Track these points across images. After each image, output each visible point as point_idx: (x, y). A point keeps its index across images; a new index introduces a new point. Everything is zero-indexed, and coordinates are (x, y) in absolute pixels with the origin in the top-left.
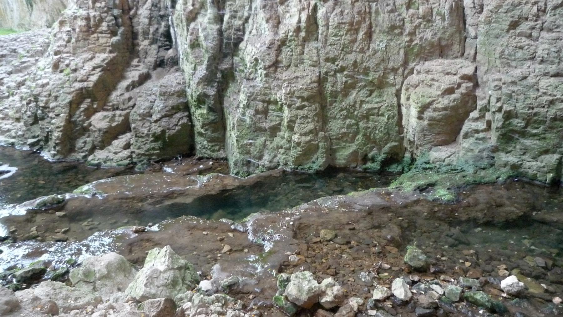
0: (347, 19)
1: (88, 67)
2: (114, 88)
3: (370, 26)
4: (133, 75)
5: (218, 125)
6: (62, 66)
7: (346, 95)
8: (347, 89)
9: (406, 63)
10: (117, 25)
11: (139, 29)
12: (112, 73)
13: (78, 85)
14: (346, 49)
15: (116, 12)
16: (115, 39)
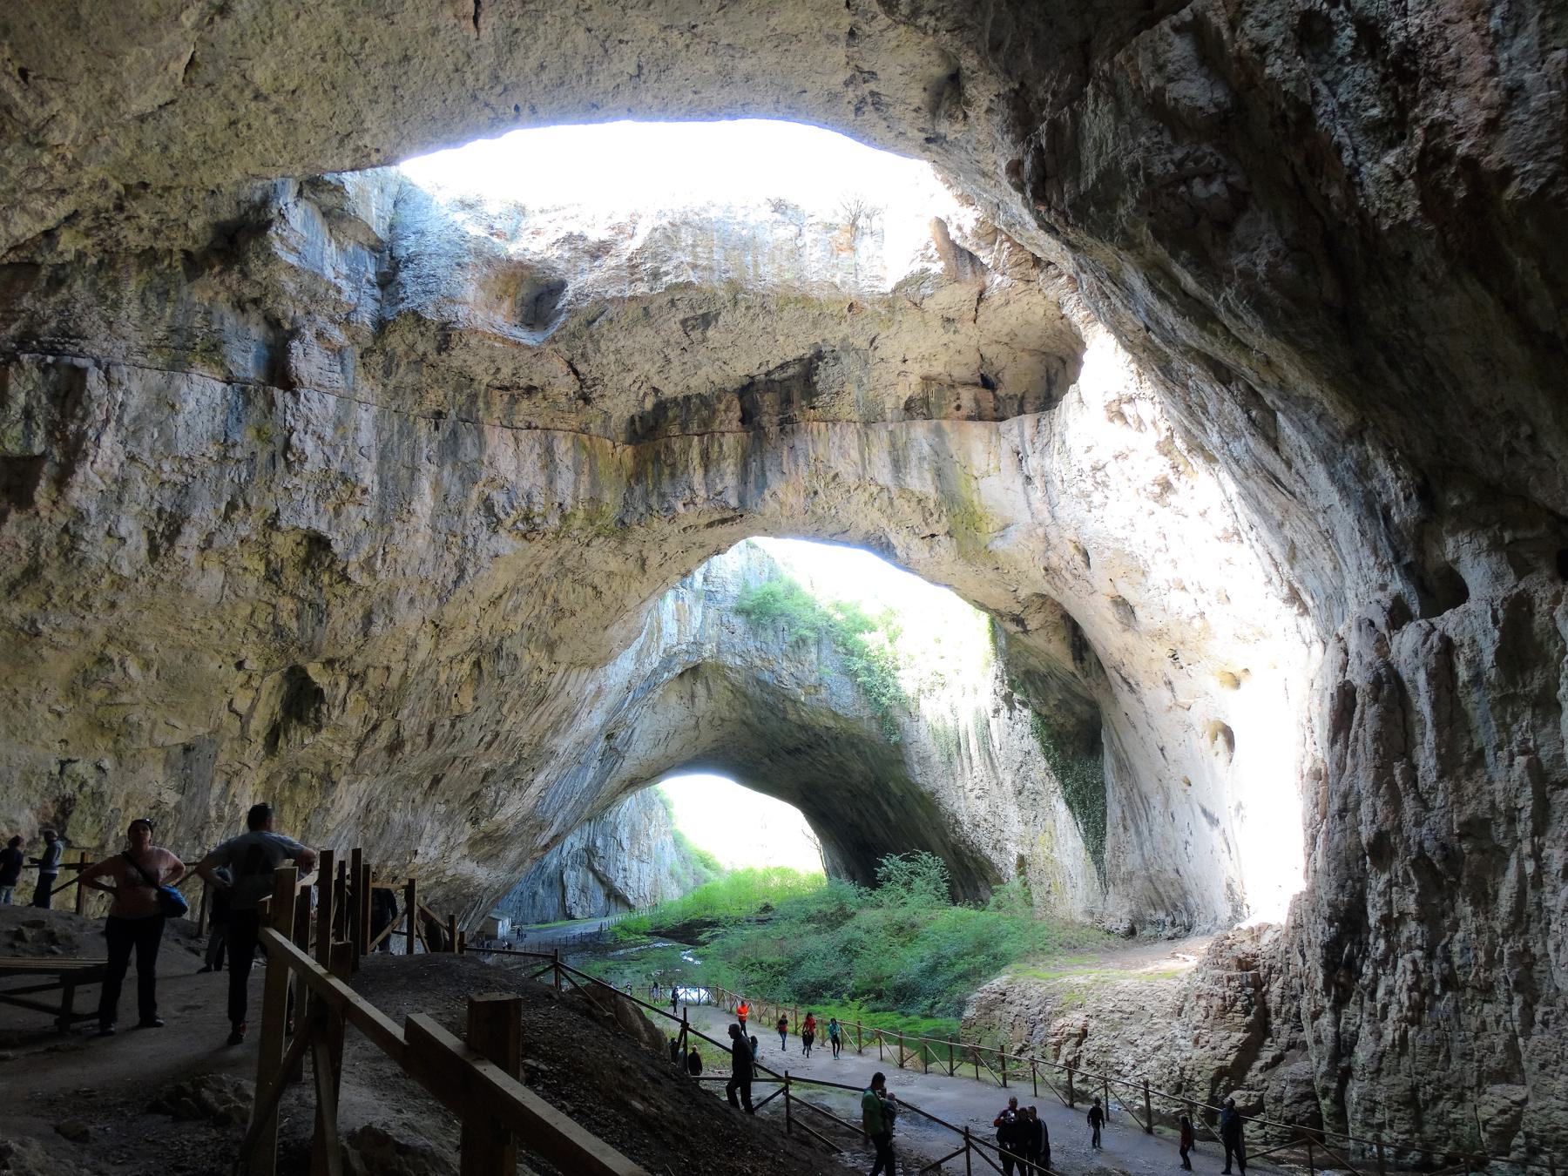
0: (1428, 1043)
1: (1226, 1045)
2: (1249, 1068)
3: (1448, 1051)
4: (1267, 1056)
5: (1340, 1115)
6: (1202, 1042)
7: (1435, 1105)
8: (1436, 1099)
9: (1479, 1084)
10: (1251, 1004)
11: (1272, 1006)
12: (1248, 1052)
13: (1218, 1063)
14: (1432, 1065)
15: (1249, 990)
16: (1249, 1019)
